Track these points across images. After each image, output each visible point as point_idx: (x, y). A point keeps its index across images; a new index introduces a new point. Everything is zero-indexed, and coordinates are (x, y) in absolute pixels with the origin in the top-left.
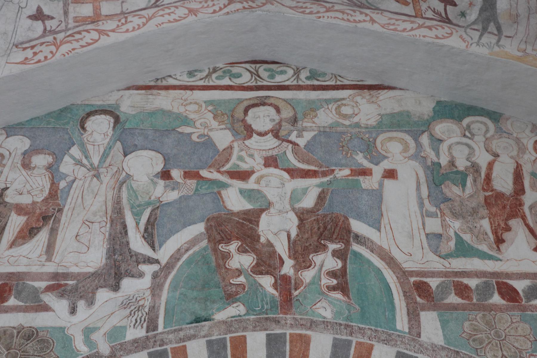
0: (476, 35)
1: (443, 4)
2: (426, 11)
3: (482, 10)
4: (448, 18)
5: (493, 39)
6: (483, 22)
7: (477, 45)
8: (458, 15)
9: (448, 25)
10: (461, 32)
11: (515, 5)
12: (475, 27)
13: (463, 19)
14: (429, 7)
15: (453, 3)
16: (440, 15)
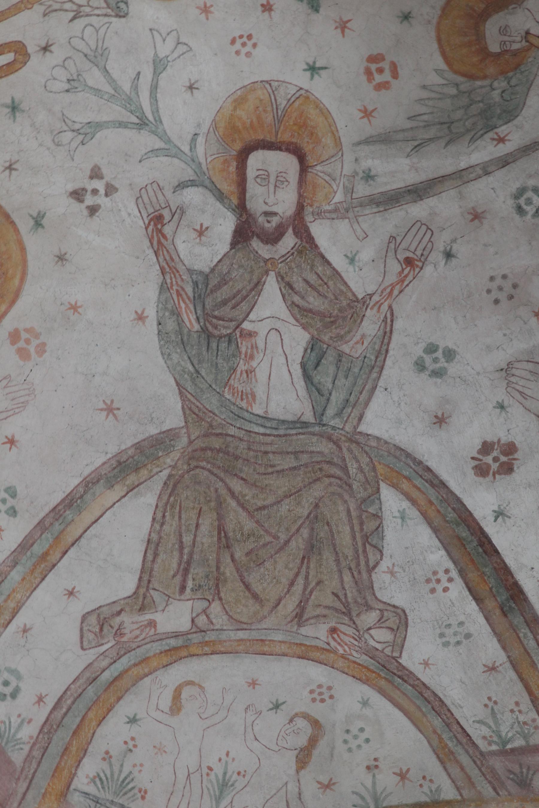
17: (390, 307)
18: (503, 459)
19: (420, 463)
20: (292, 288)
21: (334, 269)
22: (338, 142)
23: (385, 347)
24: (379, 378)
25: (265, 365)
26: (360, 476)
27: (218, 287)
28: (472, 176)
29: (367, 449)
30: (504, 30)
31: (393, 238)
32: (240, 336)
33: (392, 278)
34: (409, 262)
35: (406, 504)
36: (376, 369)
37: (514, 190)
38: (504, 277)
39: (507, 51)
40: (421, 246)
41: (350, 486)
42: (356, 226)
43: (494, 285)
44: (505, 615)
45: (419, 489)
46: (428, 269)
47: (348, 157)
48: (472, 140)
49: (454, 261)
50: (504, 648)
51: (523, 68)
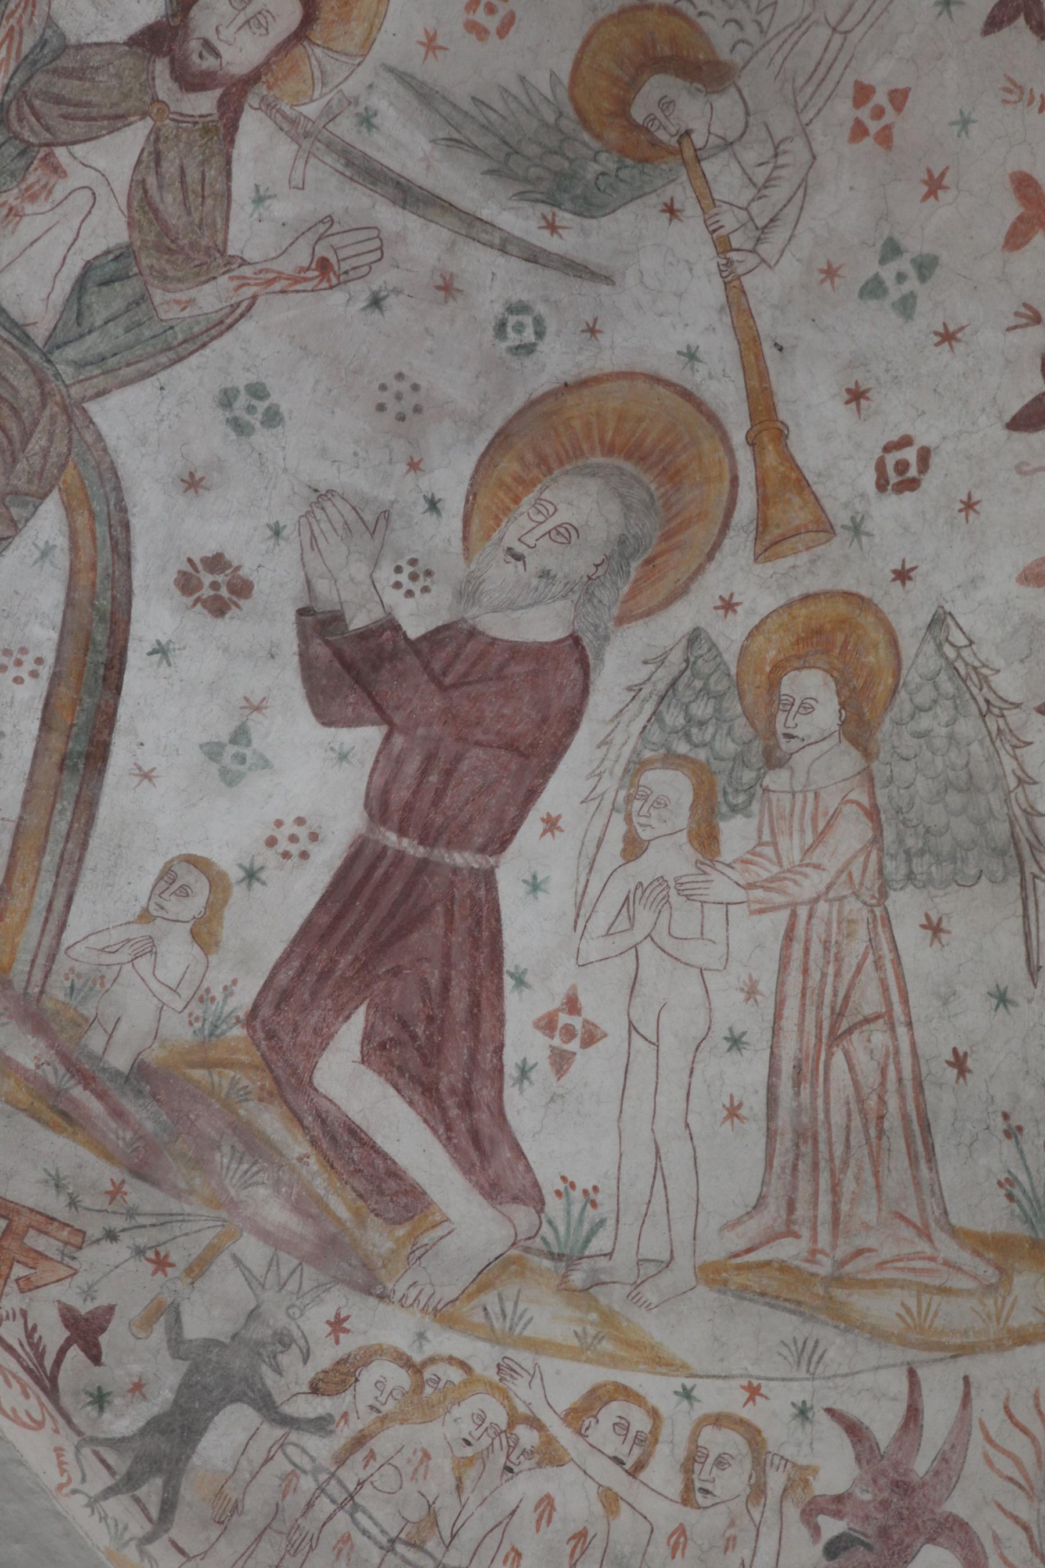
0: (101, 1480)
1: (67, 1334)
2: (8, 1317)
3: (155, 1426)
4: (53, 1379)
5: (139, 1527)
6: (137, 1460)
7: (88, 1505)
8: (87, 1393)
9: (44, 1399)
10: (67, 1440)
11: (248, 1476)
12: (111, 1458)
13: (92, 1411)
14: (24, 1314)
15: (94, 1352)
16: (40, 1356)
17: (254, 298)
18: (224, 592)
19: (124, 510)
20: (158, 163)
21: (229, 189)
22: (368, 43)
23: (205, 338)
24: (165, 367)
25: (40, 223)
26: (37, 461)
27: (68, 73)
28: (484, 237)
29: (75, 435)
30: (666, 104)
31: (330, 220)
32: (43, 159)
33: (287, 265)
34: (324, 266)
35: (62, 542)
36: (172, 355)
37: (514, 299)
38: (415, 387)
39: (648, 131)
40: (355, 262)
41: (15, 461)
42: (300, 164)
43: (395, 386)
44: (61, 767)
45: (94, 539)
46: (338, 297)
47: (364, 74)
48: (521, 196)
49: (376, 315)
50: (25, 804)
51: (648, 168)
